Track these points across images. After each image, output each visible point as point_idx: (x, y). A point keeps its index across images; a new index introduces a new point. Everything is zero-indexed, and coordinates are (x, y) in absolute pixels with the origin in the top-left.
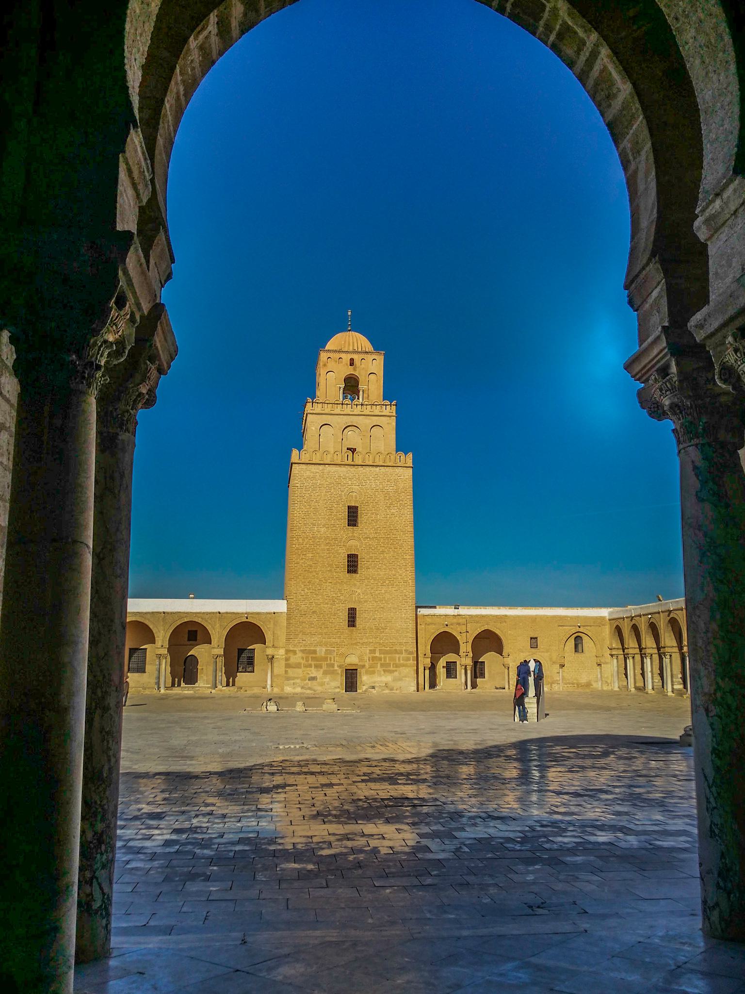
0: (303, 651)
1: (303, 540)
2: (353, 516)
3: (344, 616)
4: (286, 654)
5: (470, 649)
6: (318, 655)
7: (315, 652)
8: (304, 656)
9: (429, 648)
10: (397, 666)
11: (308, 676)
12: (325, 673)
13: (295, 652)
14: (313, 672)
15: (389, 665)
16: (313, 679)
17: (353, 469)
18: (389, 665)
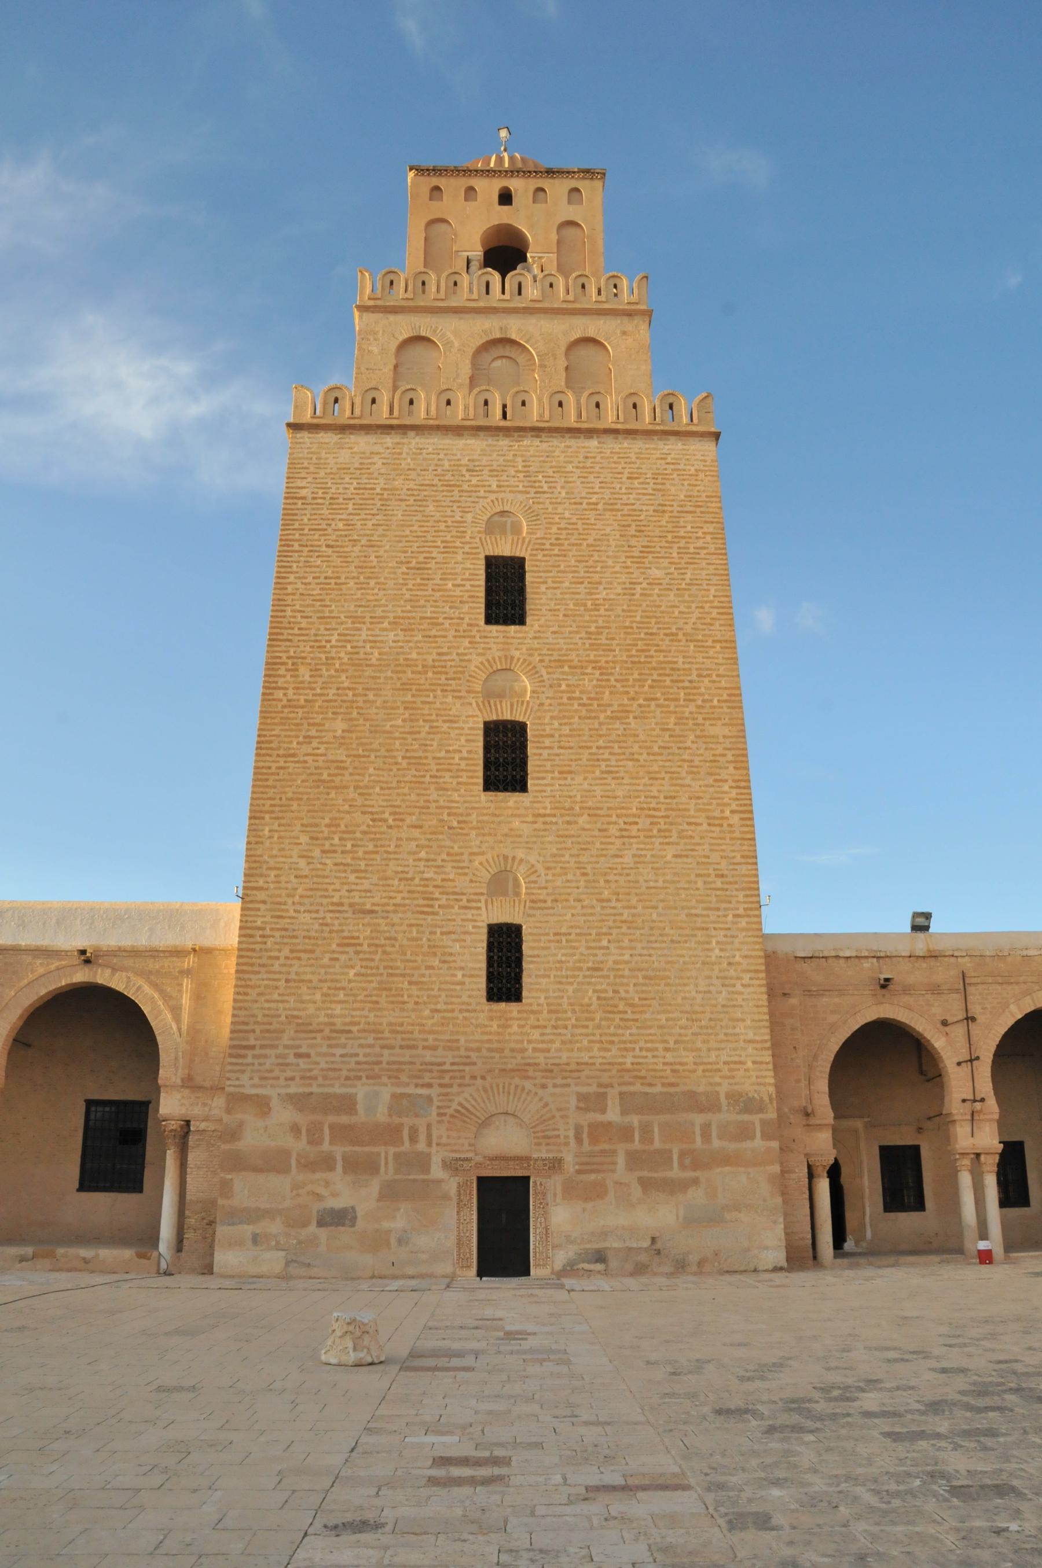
0: (298, 1101)
1: (315, 671)
2: (506, 593)
3: (473, 959)
4: (229, 1111)
5: (985, 1086)
6: (362, 1116)
7: (348, 1104)
8: (303, 1120)
9: (822, 1085)
10: (697, 1162)
11: (317, 1206)
12: (390, 1193)
13: (263, 1106)
14: (341, 1191)
15: (663, 1158)
16: (339, 1218)
17: (504, 442)
18: (663, 1158)
